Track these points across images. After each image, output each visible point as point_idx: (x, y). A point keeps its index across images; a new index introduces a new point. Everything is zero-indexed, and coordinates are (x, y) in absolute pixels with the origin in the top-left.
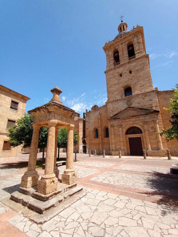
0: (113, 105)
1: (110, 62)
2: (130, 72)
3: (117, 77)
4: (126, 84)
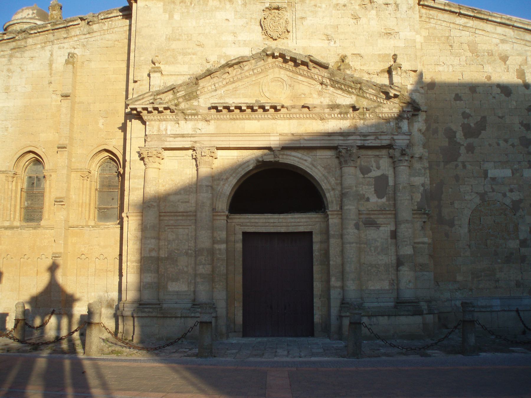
0: (177, 17)
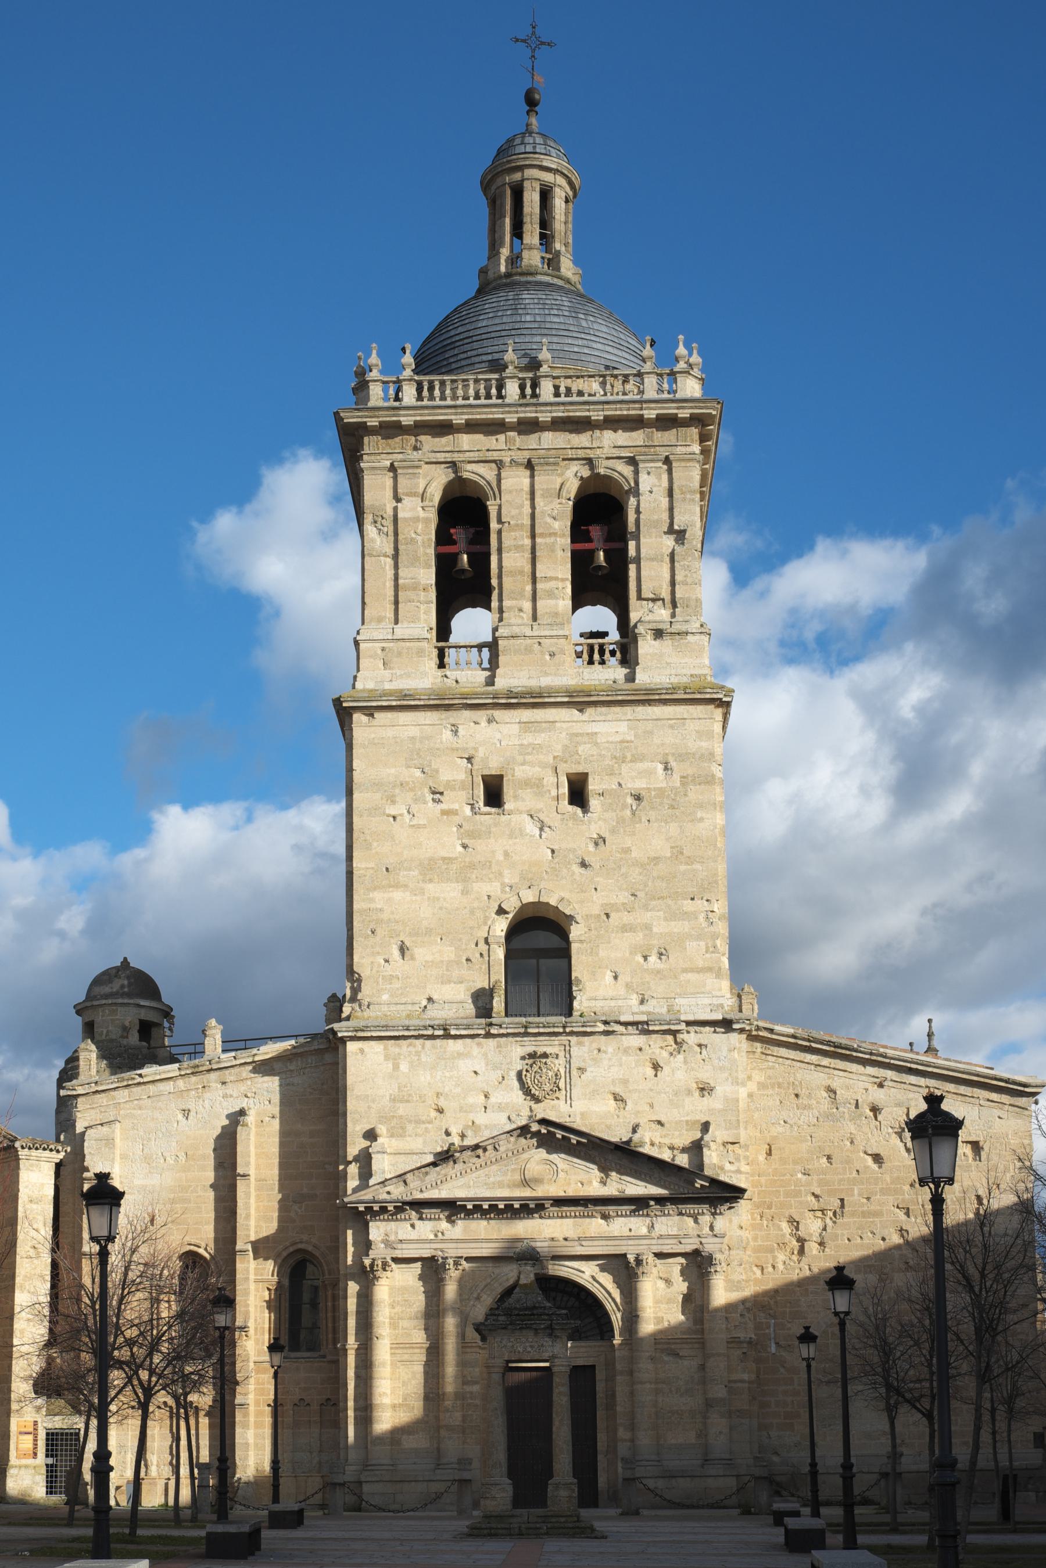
0: (404, 1067)
4: (529, 897)
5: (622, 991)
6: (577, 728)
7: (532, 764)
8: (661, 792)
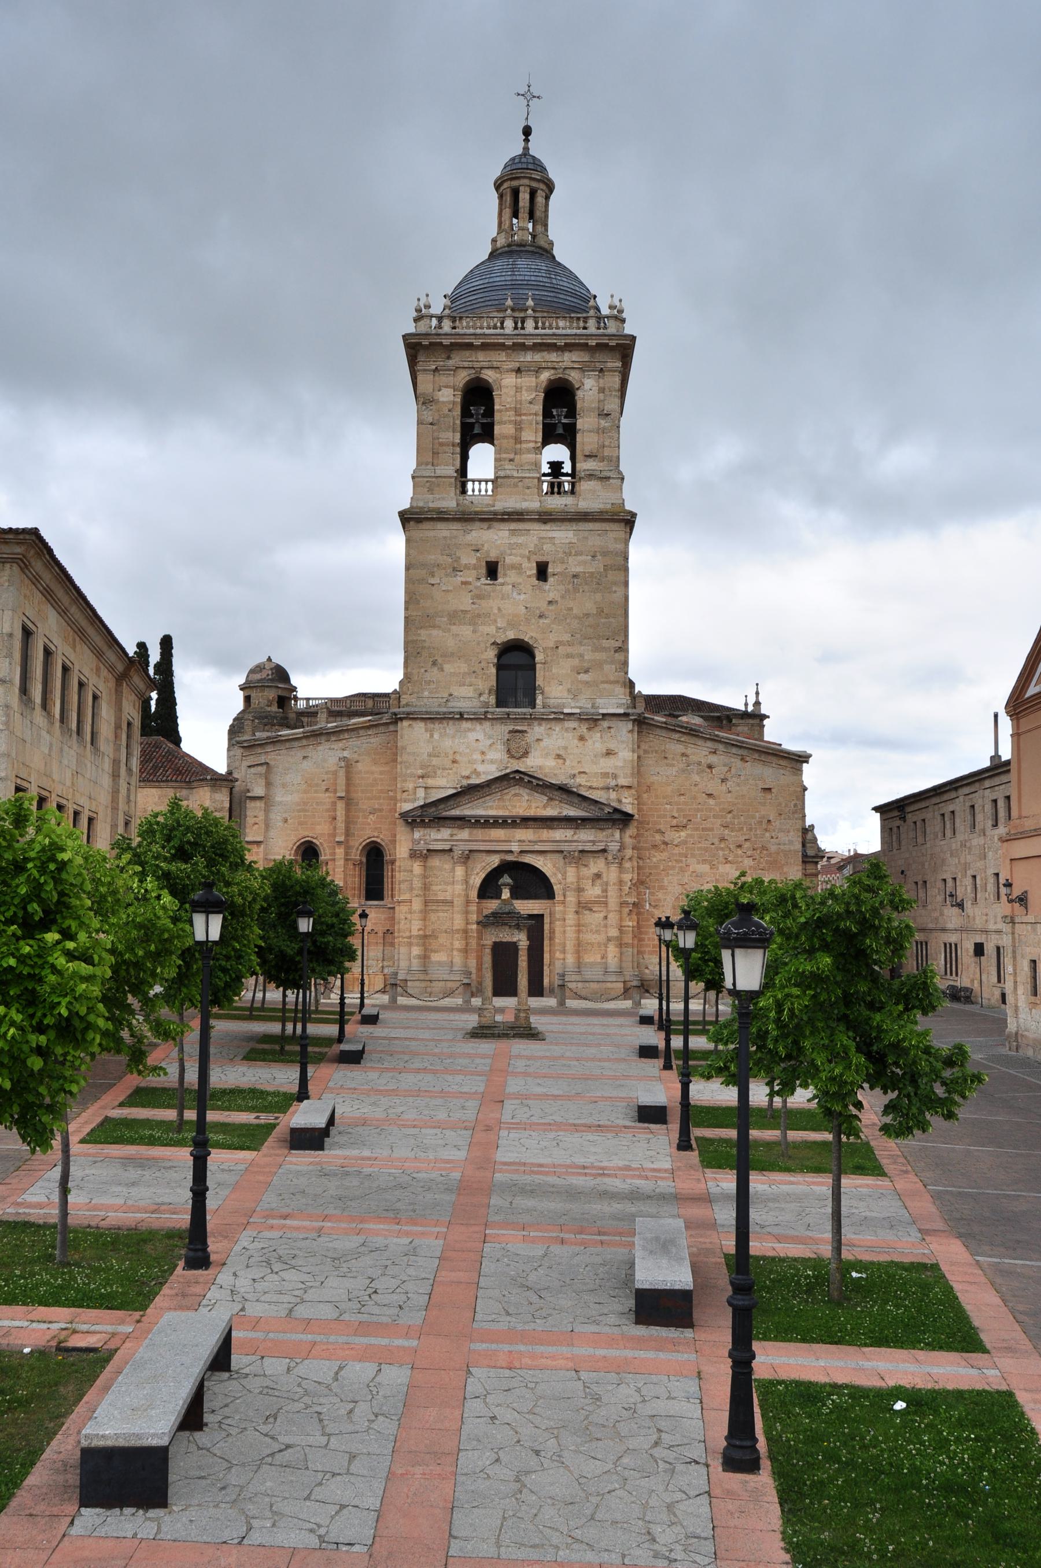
0: (436, 736)
1: (435, 454)
2: (542, 572)
3: (470, 576)
4: (511, 635)
5: (566, 694)
6: (543, 534)
7: (516, 555)
8: (592, 573)
